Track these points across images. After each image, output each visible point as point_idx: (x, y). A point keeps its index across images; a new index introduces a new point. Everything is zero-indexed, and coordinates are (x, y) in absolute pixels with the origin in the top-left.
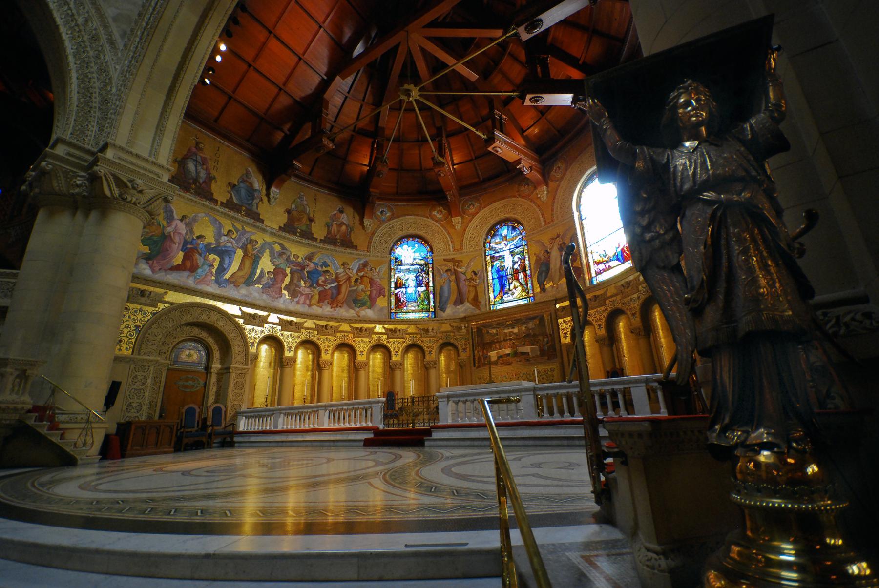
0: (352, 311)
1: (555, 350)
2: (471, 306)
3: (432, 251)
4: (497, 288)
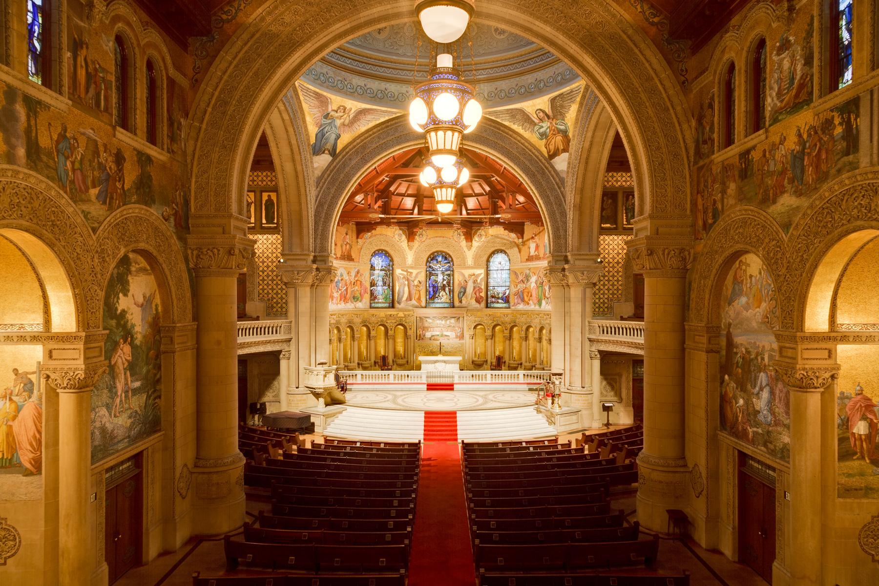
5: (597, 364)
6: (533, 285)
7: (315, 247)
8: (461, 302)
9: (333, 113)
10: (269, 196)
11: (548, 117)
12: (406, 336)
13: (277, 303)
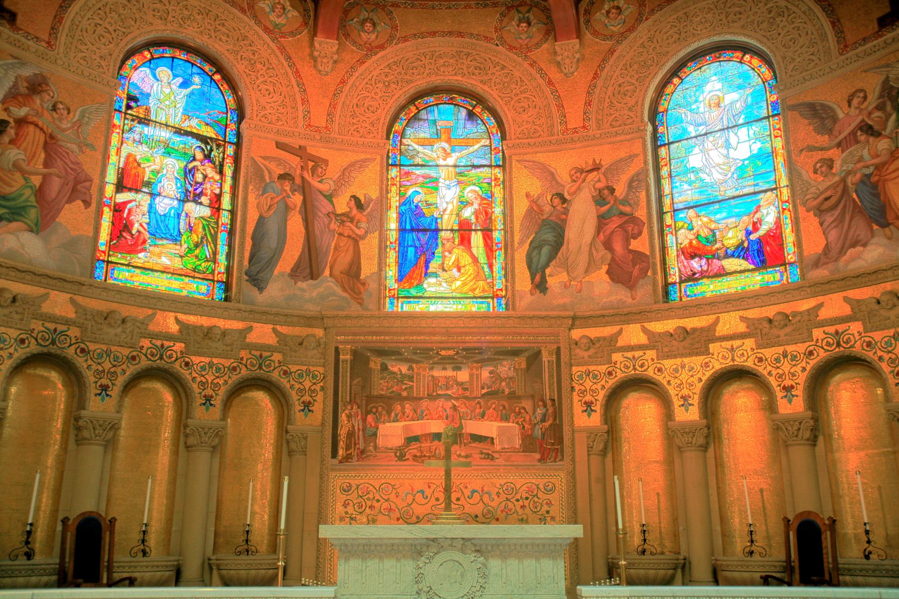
1: (560, 441)
2: (338, 290)
8: (541, 286)
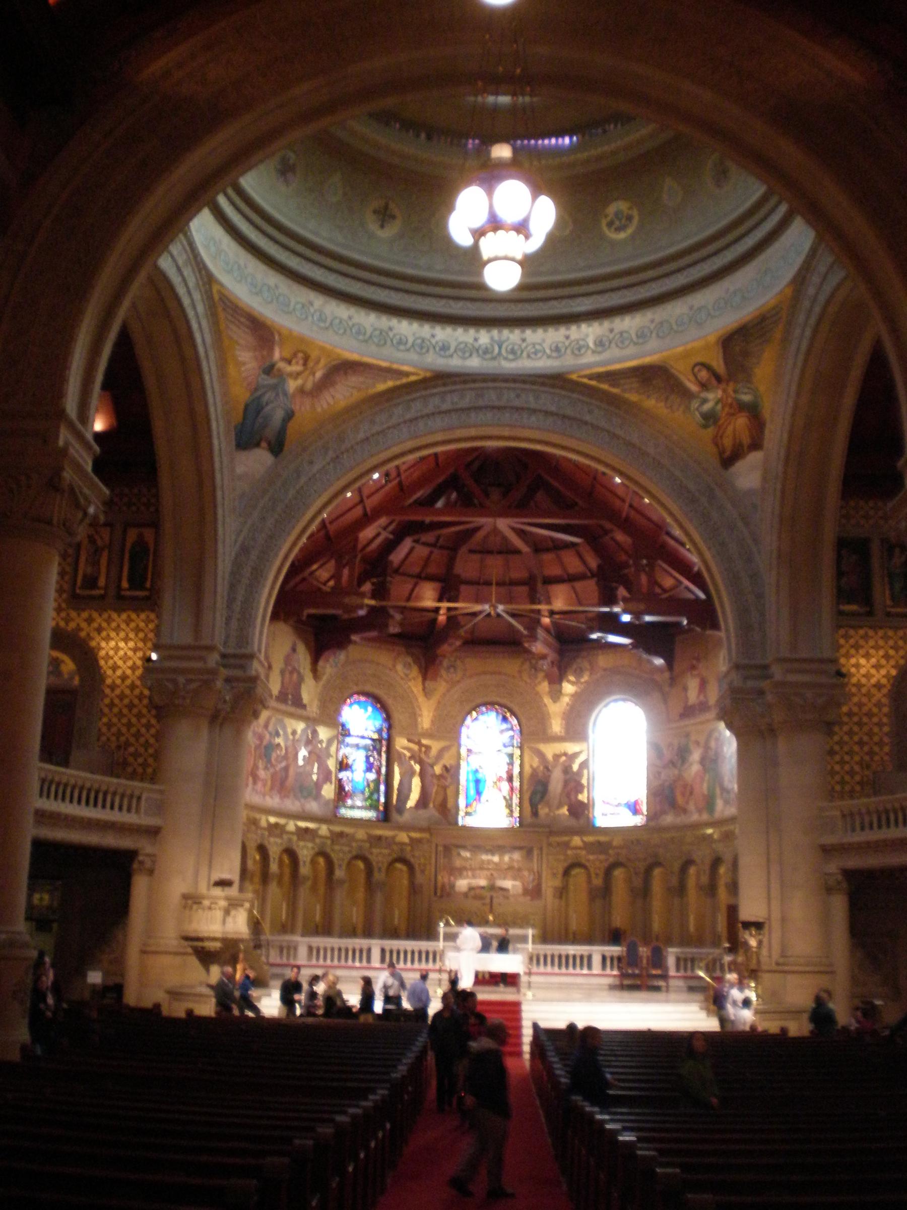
0: (297, 804)
3: (388, 719)
4: (472, 792)
5: (839, 905)
6: (695, 768)
7: (227, 637)
8: (535, 814)
9: (281, 365)
10: (141, 536)
11: (718, 379)
12: (414, 889)
13: (136, 755)
